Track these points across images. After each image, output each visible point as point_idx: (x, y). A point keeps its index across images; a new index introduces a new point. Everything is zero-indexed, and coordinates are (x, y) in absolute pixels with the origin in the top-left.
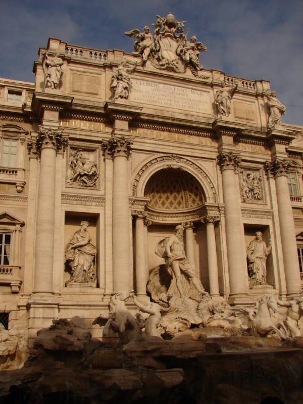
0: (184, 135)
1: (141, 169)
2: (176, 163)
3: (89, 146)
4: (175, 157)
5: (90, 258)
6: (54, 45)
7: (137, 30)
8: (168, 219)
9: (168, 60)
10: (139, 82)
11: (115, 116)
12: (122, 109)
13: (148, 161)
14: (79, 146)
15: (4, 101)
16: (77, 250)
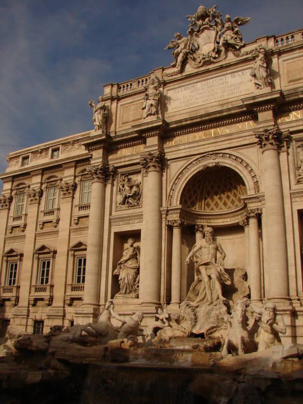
0: (181, 136)
1: (177, 177)
2: (212, 161)
3: (134, 169)
4: (212, 154)
5: (132, 272)
6: (107, 90)
7: (172, 40)
8: (229, 219)
9: (204, 55)
10: (177, 91)
11: (144, 135)
12: (146, 127)
13: (184, 167)
14: (126, 171)
15: (83, 151)
16: (122, 266)
